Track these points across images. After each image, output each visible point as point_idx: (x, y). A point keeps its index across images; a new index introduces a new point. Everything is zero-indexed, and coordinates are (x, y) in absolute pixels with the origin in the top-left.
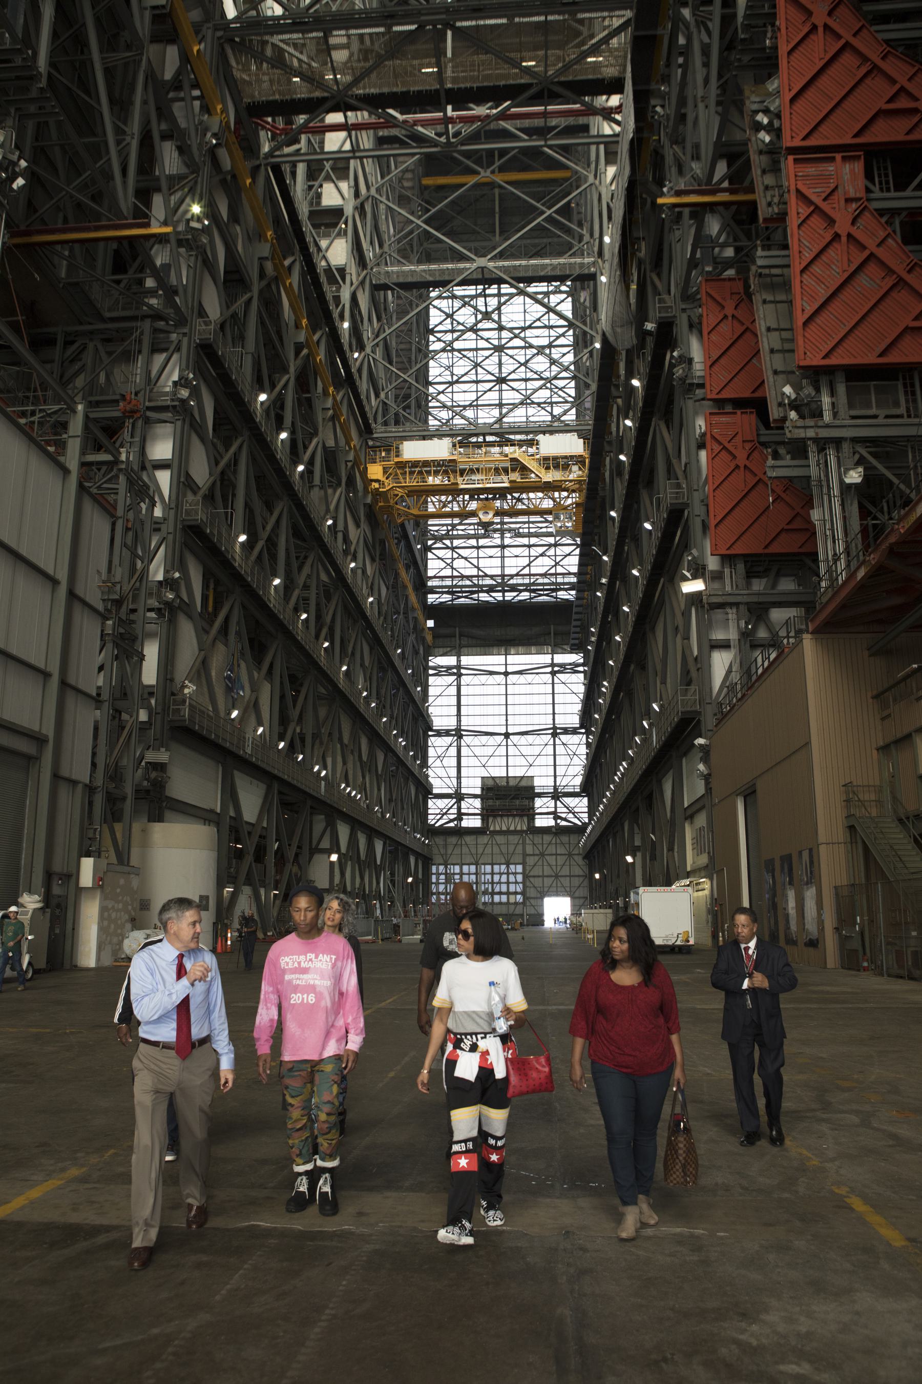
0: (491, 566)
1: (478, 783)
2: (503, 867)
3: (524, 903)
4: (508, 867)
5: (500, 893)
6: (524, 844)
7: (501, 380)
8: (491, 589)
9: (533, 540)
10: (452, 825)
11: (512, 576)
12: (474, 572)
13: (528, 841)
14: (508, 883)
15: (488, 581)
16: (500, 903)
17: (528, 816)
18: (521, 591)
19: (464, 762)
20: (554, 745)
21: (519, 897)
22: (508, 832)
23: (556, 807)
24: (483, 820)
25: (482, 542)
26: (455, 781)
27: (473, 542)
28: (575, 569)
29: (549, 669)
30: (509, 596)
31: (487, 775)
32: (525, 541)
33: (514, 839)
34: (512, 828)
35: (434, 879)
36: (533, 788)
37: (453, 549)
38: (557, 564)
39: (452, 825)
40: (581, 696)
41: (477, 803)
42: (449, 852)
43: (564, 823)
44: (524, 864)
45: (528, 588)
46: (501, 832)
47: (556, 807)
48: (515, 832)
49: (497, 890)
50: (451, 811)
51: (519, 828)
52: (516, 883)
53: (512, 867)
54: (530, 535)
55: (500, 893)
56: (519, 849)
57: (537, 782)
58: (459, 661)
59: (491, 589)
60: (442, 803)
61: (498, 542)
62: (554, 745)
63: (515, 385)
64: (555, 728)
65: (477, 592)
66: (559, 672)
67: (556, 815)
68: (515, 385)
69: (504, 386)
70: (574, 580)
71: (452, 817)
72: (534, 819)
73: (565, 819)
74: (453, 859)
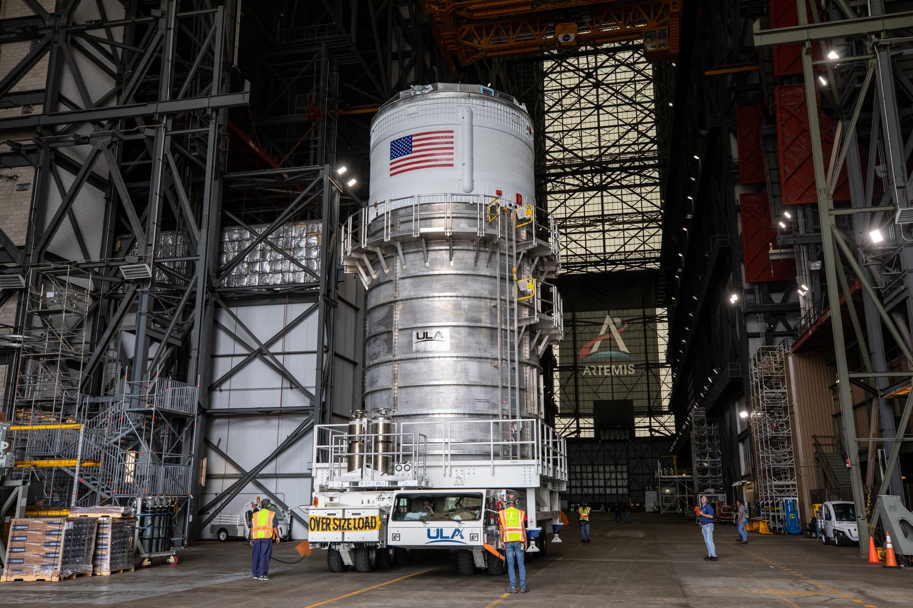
0: (596, 247)
1: (591, 404)
2: (612, 467)
3: (629, 495)
4: (616, 467)
5: (611, 487)
7: (598, 107)
8: (596, 264)
9: (626, 226)
10: (573, 436)
11: (613, 254)
12: (583, 251)
14: (616, 479)
15: (594, 259)
16: (611, 494)
18: (617, 265)
19: (580, 389)
20: (648, 376)
21: (625, 489)
22: (615, 441)
23: (650, 422)
24: (595, 432)
25: (588, 229)
26: (574, 403)
27: (582, 229)
28: (658, 246)
29: (641, 320)
30: (609, 268)
31: (597, 399)
32: (621, 227)
34: (618, 438)
37: (566, 234)
38: (644, 243)
39: (573, 436)
40: (667, 339)
43: (657, 434)
44: (628, 464)
45: (625, 262)
46: (609, 441)
47: (650, 422)
48: (620, 441)
49: (608, 484)
50: (572, 426)
51: (623, 438)
52: (623, 479)
54: (624, 223)
55: (611, 487)
57: (635, 404)
58: (574, 316)
59: (596, 264)
60: (565, 421)
61: (601, 228)
62: (648, 376)
63: (609, 109)
64: (647, 364)
65: (587, 266)
66: (649, 322)
67: (651, 428)
68: (609, 109)
69: (601, 111)
70: (658, 255)
71: (573, 430)
72: (634, 431)
73: (658, 431)
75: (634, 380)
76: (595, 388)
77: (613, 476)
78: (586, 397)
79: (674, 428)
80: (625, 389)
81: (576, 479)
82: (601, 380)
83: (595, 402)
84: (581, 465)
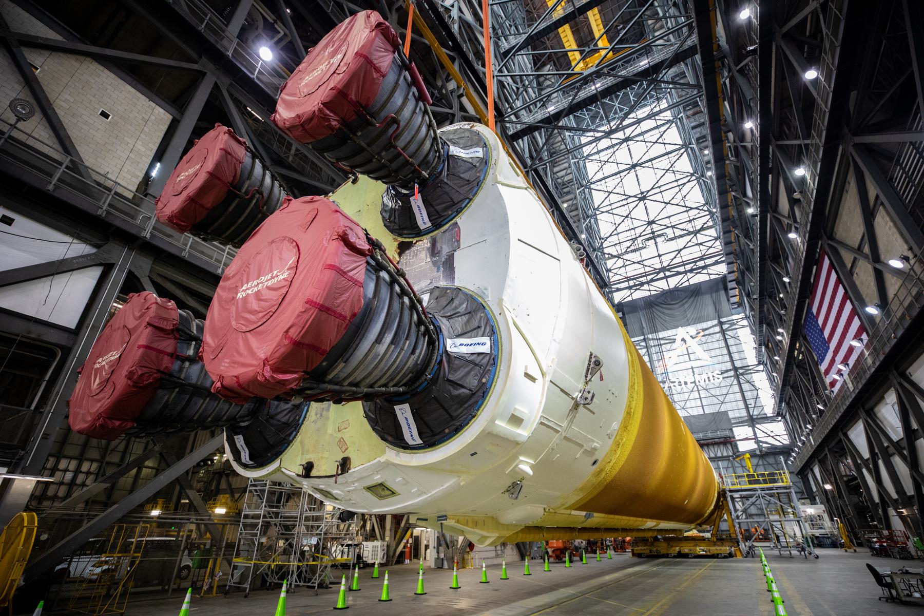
17: (731, 443)
31: (687, 415)
36: (730, 420)
43: (764, 445)
48: (722, 458)
51: (725, 454)
57: (731, 415)
64: (735, 369)
75: (724, 391)
79: (786, 437)
80: (716, 401)
82: (686, 395)
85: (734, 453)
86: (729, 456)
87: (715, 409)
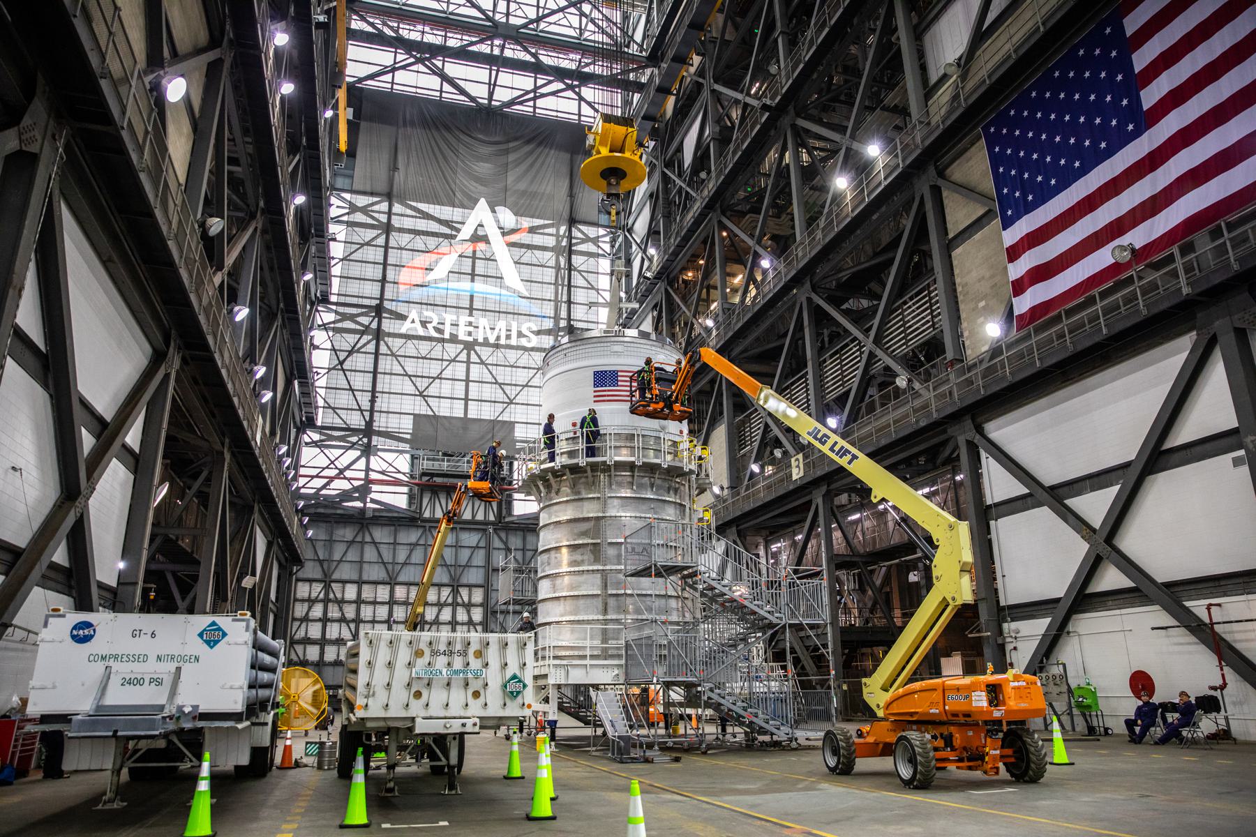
1: (407, 425)
2: (446, 592)
6: (488, 549)
13: (497, 543)
24: (411, 497)
31: (424, 410)
33: (471, 539)
35: (300, 610)
41: (403, 463)
42: (337, 557)
48: (472, 526)
51: (480, 517)
52: (470, 623)
53: (464, 592)
56: (479, 559)
57: (520, 432)
74: (345, 572)
76: (422, 384)
77: (446, 615)
78: (395, 404)
81: (343, 620)
83: (417, 418)
84: (360, 583)
85: (499, 516)
86: (486, 523)
87: (487, 412)
